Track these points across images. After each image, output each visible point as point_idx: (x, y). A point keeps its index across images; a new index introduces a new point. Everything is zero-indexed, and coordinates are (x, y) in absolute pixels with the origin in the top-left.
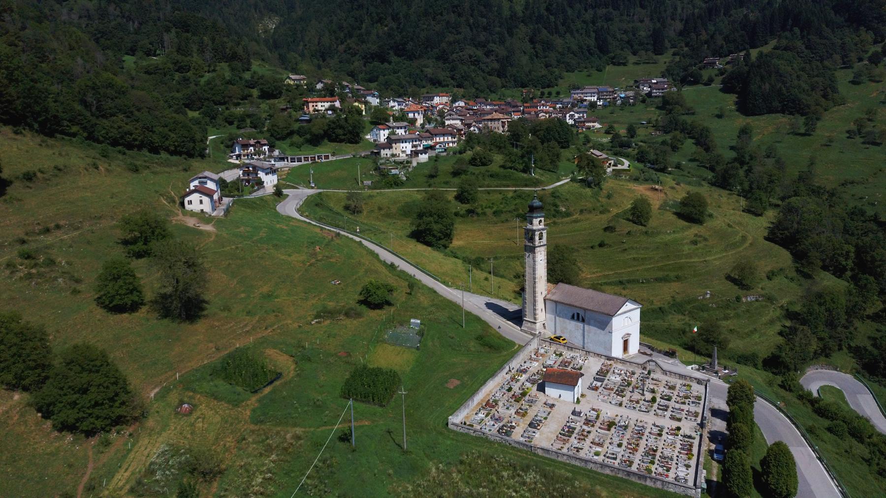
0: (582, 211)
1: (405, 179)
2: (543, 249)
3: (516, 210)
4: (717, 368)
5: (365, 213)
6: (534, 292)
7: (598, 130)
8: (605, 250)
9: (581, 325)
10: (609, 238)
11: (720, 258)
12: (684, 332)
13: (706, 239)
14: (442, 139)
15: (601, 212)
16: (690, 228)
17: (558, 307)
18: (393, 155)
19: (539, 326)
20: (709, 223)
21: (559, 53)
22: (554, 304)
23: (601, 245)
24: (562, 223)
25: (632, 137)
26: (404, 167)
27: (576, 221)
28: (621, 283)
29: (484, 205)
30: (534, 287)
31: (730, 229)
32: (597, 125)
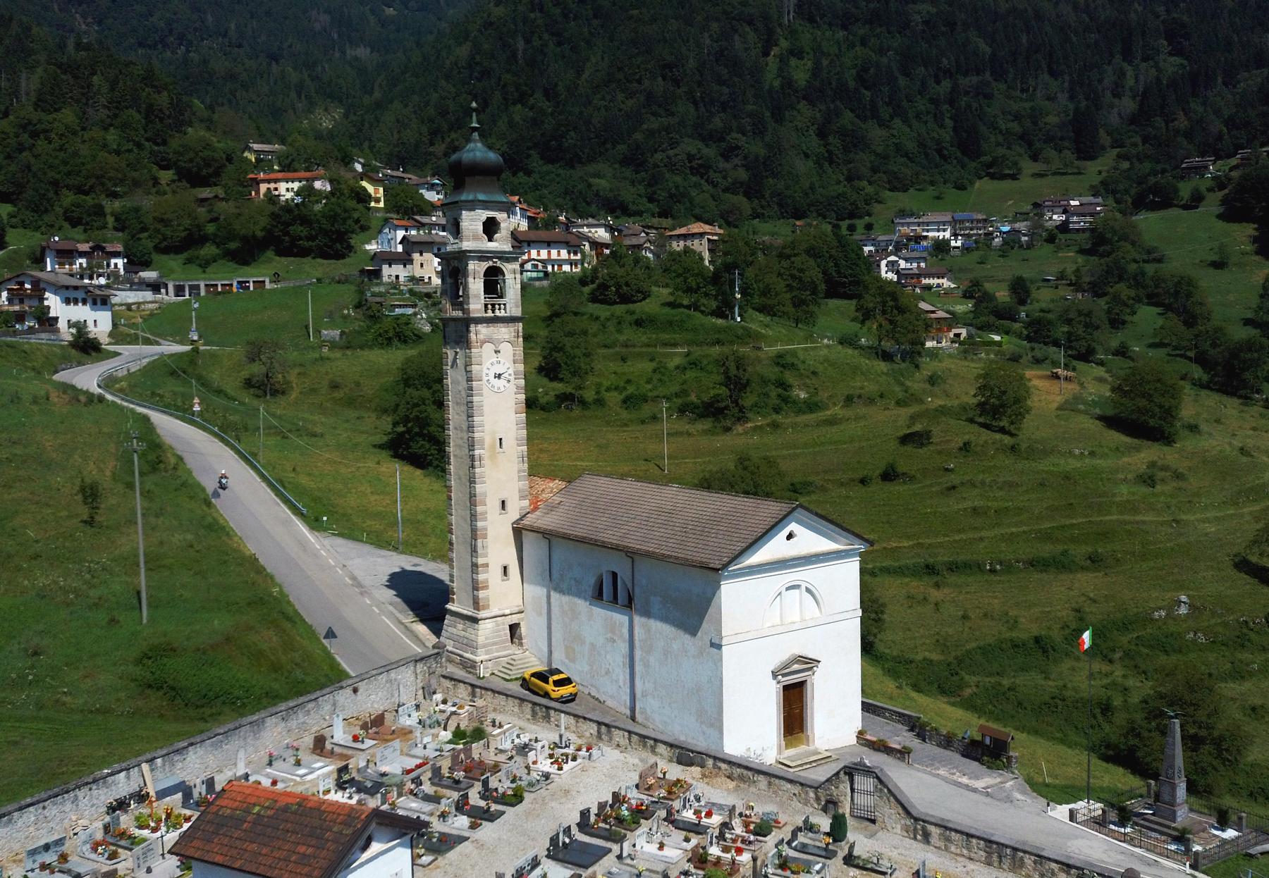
0: (849, 400)
1: (428, 328)
2: (504, 332)
3: (684, 393)
4: (1183, 816)
6: (472, 499)
7: (948, 292)
8: (897, 488)
9: (621, 619)
10: (909, 460)
11: (1217, 519)
12: (1106, 709)
13: (1179, 476)
14: (544, 254)
15: (899, 403)
16: (1138, 449)
17: (559, 554)
18: (412, 279)
19: (488, 631)
20: (1188, 443)
21: (877, 155)
22: (544, 543)
23: (889, 475)
24: (794, 426)
25: (1022, 302)
26: (434, 304)
27: (832, 422)
28: (930, 569)
29: (606, 383)
30: (472, 481)
31: (1245, 459)
32: (946, 283)
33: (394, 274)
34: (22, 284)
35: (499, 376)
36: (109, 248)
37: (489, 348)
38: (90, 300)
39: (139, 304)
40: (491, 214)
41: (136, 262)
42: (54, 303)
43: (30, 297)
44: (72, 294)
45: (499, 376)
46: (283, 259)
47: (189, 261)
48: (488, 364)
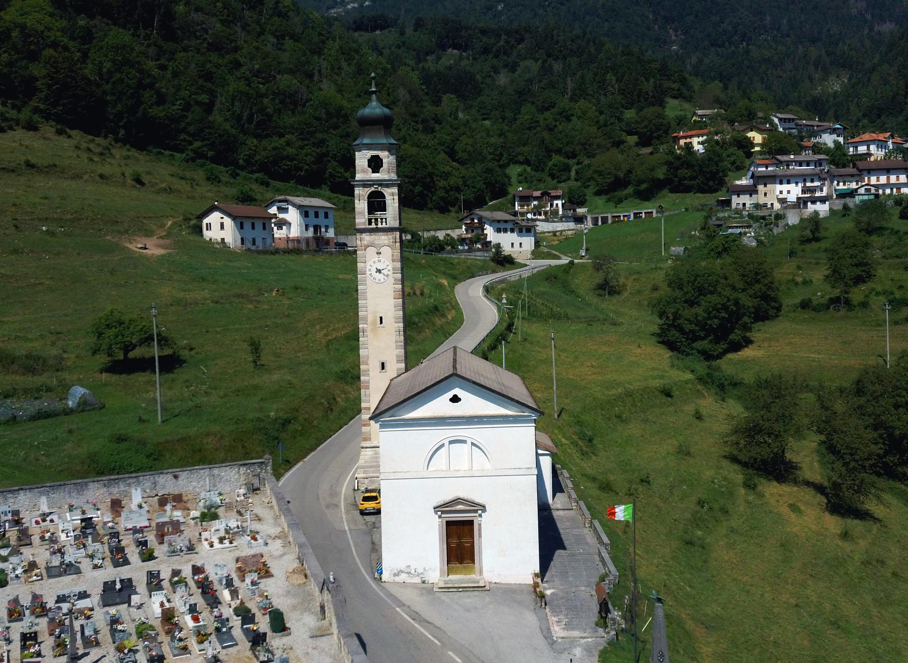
5: (626, 294)
14: (883, 179)
18: (757, 206)
33: (741, 202)
34: (473, 220)
35: (379, 271)
36: (553, 193)
37: (371, 251)
38: (517, 230)
39: (562, 231)
40: (375, 153)
41: (574, 201)
42: (489, 230)
43: (477, 228)
44: (502, 226)
45: (379, 271)
46: (673, 195)
47: (608, 200)
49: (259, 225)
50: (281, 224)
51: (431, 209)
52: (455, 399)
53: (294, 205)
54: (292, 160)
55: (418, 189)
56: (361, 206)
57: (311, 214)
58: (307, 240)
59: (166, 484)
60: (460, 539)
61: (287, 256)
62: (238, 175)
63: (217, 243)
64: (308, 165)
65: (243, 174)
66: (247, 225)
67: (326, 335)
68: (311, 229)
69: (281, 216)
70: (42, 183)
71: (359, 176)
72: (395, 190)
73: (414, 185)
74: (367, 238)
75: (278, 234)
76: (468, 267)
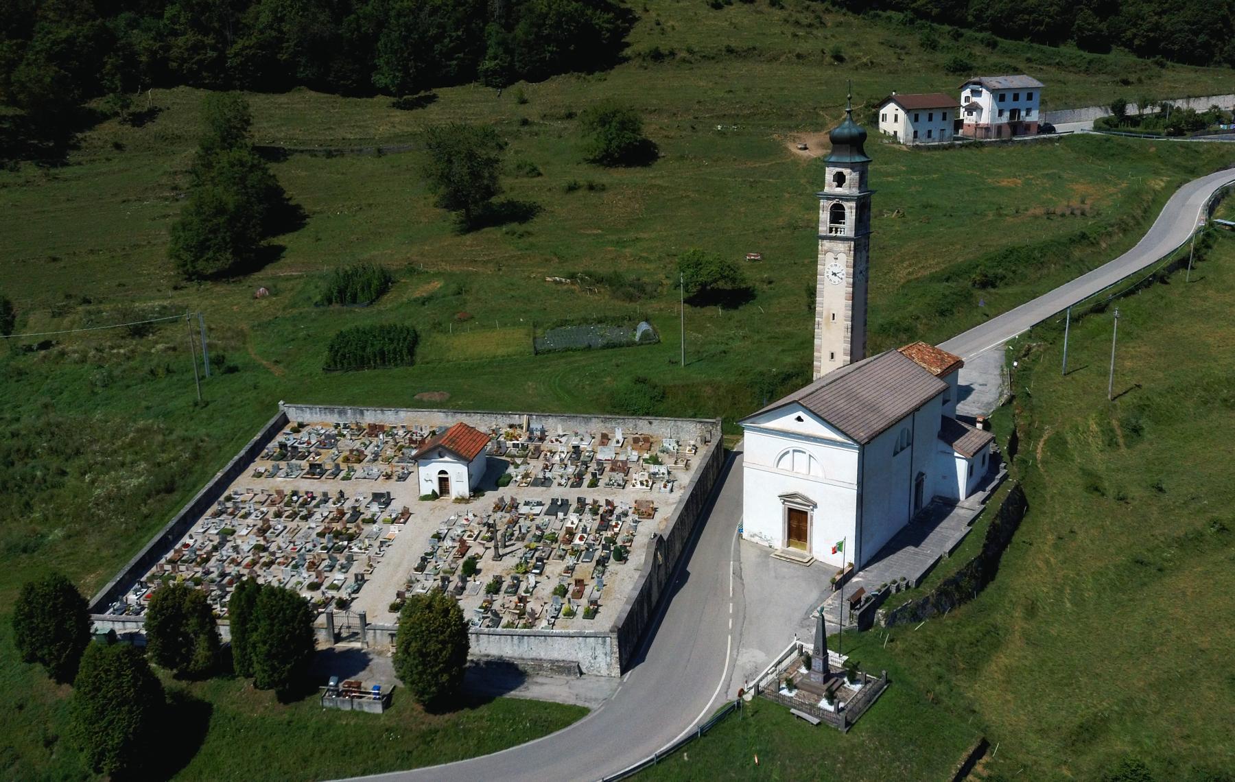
2: (841, 246)
35: (834, 274)
37: (830, 256)
45: (834, 274)
48: (827, 266)
49: (937, 117)
50: (973, 108)
51: (1219, 63)
52: (799, 419)
53: (988, 89)
54: (1030, 13)
55: (1202, 38)
56: (825, 216)
57: (1009, 97)
58: (999, 127)
59: (643, 427)
60: (797, 524)
61: (965, 152)
62: (962, 35)
63: (890, 137)
64: (1050, 17)
65: (968, 33)
66: (923, 117)
67: (909, 273)
68: (1007, 114)
69: (974, 99)
70: (739, 69)
71: (827, 190)
72: (853, 204)
73: (1196, 33)
74: (826, 244)
75: (968, 120)
76: (1223, 156)
